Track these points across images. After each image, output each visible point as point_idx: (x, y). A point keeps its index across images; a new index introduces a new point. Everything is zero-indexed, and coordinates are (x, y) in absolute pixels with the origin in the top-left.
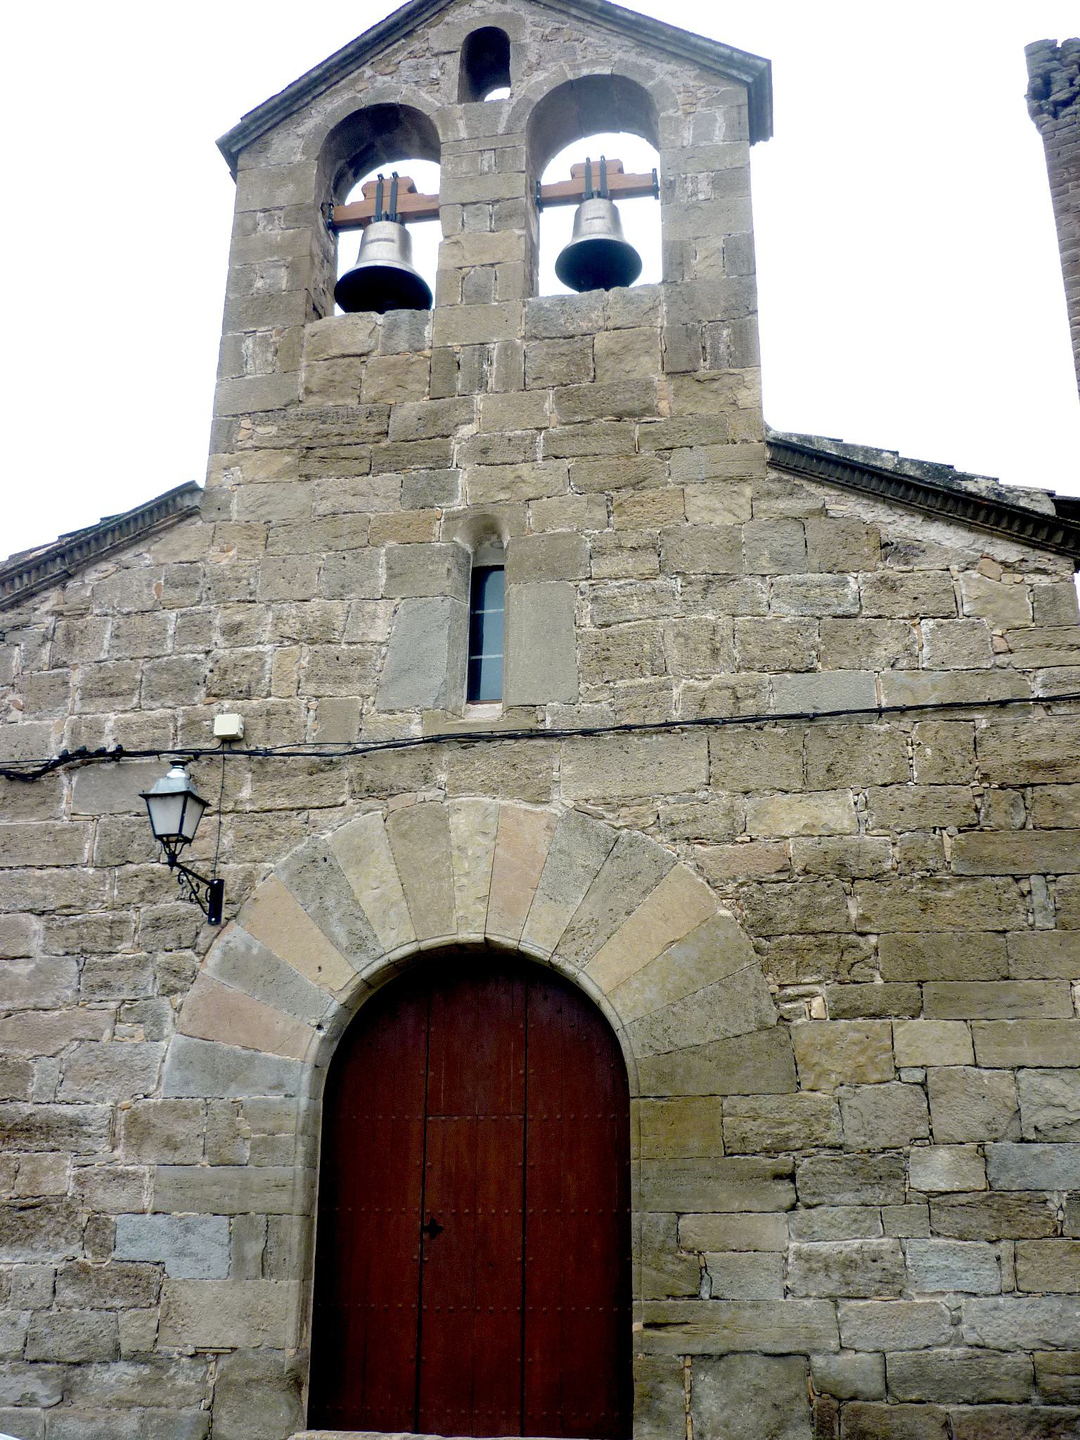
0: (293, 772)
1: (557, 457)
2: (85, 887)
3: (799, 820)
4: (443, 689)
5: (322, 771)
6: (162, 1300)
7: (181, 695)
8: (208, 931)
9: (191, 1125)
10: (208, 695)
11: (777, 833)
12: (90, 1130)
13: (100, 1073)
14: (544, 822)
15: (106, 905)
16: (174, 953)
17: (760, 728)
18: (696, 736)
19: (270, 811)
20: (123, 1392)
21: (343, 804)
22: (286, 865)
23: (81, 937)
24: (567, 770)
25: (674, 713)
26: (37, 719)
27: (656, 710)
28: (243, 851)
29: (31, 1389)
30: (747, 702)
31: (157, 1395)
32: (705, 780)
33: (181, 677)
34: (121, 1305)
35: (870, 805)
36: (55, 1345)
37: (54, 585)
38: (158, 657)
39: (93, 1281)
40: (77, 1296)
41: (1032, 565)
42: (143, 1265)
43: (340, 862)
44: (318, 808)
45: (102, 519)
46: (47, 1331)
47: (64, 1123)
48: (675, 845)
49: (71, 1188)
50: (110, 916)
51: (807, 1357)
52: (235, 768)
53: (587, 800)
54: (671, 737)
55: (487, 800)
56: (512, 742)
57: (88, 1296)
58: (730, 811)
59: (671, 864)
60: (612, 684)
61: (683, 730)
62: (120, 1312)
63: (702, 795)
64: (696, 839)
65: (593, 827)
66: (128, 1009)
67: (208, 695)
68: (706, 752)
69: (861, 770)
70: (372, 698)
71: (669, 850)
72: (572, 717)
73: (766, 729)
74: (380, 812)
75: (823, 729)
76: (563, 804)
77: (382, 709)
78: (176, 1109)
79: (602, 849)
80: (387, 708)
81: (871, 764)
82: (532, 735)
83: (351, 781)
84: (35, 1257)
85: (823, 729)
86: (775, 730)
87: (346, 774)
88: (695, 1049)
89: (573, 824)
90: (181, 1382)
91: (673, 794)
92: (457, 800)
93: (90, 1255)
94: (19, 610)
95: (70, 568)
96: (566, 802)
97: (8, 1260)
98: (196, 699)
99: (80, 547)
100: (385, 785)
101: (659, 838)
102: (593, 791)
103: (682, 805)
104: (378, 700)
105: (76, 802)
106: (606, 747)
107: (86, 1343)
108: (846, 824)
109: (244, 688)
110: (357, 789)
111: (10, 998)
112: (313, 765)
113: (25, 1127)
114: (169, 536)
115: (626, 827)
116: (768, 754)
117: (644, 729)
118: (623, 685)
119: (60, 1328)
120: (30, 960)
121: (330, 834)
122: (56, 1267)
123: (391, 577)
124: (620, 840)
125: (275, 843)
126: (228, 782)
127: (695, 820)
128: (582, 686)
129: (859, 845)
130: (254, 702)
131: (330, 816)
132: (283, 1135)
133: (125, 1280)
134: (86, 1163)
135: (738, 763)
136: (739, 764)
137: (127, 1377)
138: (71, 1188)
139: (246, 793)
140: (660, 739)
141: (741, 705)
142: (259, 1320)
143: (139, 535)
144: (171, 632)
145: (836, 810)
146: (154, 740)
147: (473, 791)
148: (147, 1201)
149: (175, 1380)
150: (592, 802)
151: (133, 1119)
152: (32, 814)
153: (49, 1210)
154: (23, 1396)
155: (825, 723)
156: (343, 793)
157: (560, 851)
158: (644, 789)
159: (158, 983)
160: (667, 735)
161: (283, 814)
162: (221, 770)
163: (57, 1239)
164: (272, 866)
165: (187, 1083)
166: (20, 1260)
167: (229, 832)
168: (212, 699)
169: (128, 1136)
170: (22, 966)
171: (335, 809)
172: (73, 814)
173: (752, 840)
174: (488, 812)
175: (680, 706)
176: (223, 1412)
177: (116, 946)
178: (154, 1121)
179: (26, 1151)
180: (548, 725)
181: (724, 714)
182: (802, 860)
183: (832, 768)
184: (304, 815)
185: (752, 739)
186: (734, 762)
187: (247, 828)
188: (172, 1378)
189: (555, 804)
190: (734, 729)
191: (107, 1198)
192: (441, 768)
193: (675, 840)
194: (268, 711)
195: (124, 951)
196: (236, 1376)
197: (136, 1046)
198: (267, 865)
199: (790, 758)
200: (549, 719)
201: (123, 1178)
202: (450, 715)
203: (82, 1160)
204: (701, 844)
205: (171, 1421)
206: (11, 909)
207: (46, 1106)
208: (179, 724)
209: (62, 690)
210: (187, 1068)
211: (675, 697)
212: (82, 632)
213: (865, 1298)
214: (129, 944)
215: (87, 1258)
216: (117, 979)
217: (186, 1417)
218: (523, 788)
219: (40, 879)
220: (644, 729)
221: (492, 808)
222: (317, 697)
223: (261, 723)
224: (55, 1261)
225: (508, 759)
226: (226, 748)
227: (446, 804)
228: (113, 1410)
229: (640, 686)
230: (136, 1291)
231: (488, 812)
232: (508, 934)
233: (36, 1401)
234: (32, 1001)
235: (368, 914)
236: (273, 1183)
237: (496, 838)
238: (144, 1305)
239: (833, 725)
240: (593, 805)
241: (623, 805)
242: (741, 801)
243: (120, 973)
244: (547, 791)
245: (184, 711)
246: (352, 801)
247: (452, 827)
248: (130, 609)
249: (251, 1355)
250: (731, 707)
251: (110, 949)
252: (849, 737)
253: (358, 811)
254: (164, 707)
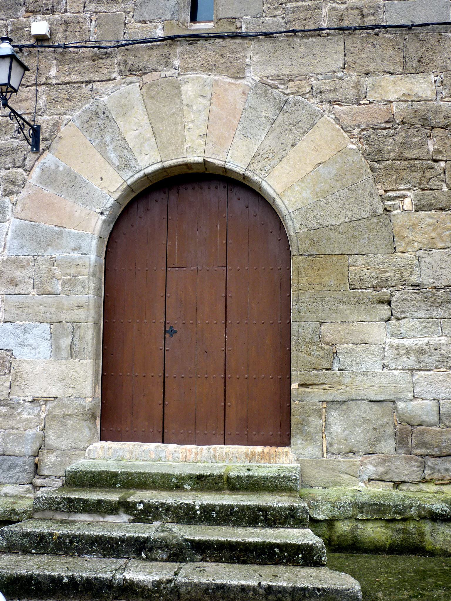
0: (82, 59)
3: (400, 90)
4: (177, 8)
5: (101, 58)
6: (12, 370)
7: (9, 12)
8: (31, 157)
10: (27, 11)
11: (386, 99)
14: (241, 90)
17: (376, 34)
18: (336, 38)
19: (68, 83)
21: (115, 79)
22: (79, 116)
24: (256, 58)
25: (323, 23)
27: (312, 22)
28: (52, 108)
30: (369, 18)
31: (12, 423)
32: (342, 65)
35: (444, 82)
43: (113, 114)
44: (98, 81)
48: (322, 105)
51: (394, 402)
52: (45, 57)
53: (268, 77)
54: (321, 39)
55: (205, 76)
56: (221, 40)
58: (357, 85)
59: (320, 116)
60: (284, 5)
61: (328, 34)
63: (340, 74)
64: (335, 102)
65: (271, 93)
67: (27, 11)
68: (343, 48)
69: (440, 62)
70: (131, 14)
71: (318, 108)
72: (259, 26)
73: (381, 34)
74: (138, 84)
75: (417, 35)
76: (253, 79)
77: (138, 19)
79: (277, 107)
80: (141, 19)
81: (446, 57)
82: (234, 36)
83: (119, 65)
85: (417, 35)
86: (386, 35)
87: (116, 61)
89: (259, 91)
90: (25, 416)
91: (321, 74)
92: (186, 76)
96: (254, 78)
98: (19, 14)
100: (141, 67)
101: (312, 101)
102: (271, 71)
103: (327, 81)
104: (135, 14)
106: (280, 44)
108: (429, 94)
109: (50, 7)
110: (123, 69)
112: (95, 54)
115: (292, 93)
116: (381, 50)
117: (305, 33)
118: (291, 6)
121: (106, 98)
124: (289, 101)
125: (72, 103)
126: (41, 65)
127: (335, 90)
128: (265, 6)
129: (437, 107)
130: (57, 16)
131: (106, 86)
132: (81, 277)
135: (363, 56)
136: (363, 56)
139: (53, 72)
140: (314, 40)
141: (366, 19)
142: (70, 382)
145: (423, 85)
147: (196, 70)
149: (22, 415)
150: (271, 78)
155: (417, 31)
156: (115, 72)
157: (251, 108)
158: (303, 70)
160: (318, 37)
161: (76, 85)
162: (37, 58)
164: (71, 117)
165: (22, 247)
167: (43, 96)
168: (29, 14)
171: (110, 82)
173: (370, 103)
174: (206, 83)
175: (327, 19)
176: (50, 432)
180: (244, 30)
181: (355, 25)
182: (401, 115)
183: (422, 59)
184: (90, 86)
185: (372, 40)
186: (360, 55)
187: (54, 94)
189: (247, 79)
190: (360, 34)
192: (176, 57)
193: (322, 102)
194: (65, 21)
196: (57, 412)
198: (67, 117)
199: (395, 53)
200: (244, 27)
202: (181, 25)
204: (338, 105)
208: (9, 30)
210: (21, 238)
211: (324, 14)
213: (429, 370)
217: (29, 435)
218: (228, 69)
220: (305, 33)
221: (208, 81)
222: (96, 13)
223: (62, 29)
225: (218, 51)
226: (39, 44)
227: (179, 79)
229: (302, 7)
231: (206, 83)
232: (218, 158)
235: (131, 146)
236: (76, 305)
237: (211, 99)
239: (423, 33)
240: (272, 80)
241: (290, 80)
242: (363, 79)
244: (243, 71)
245: (12, 22)
246: (120, 77)
247: (183, 93)
250: (359, 20)
252: (433, 41)
253: (124, 83)
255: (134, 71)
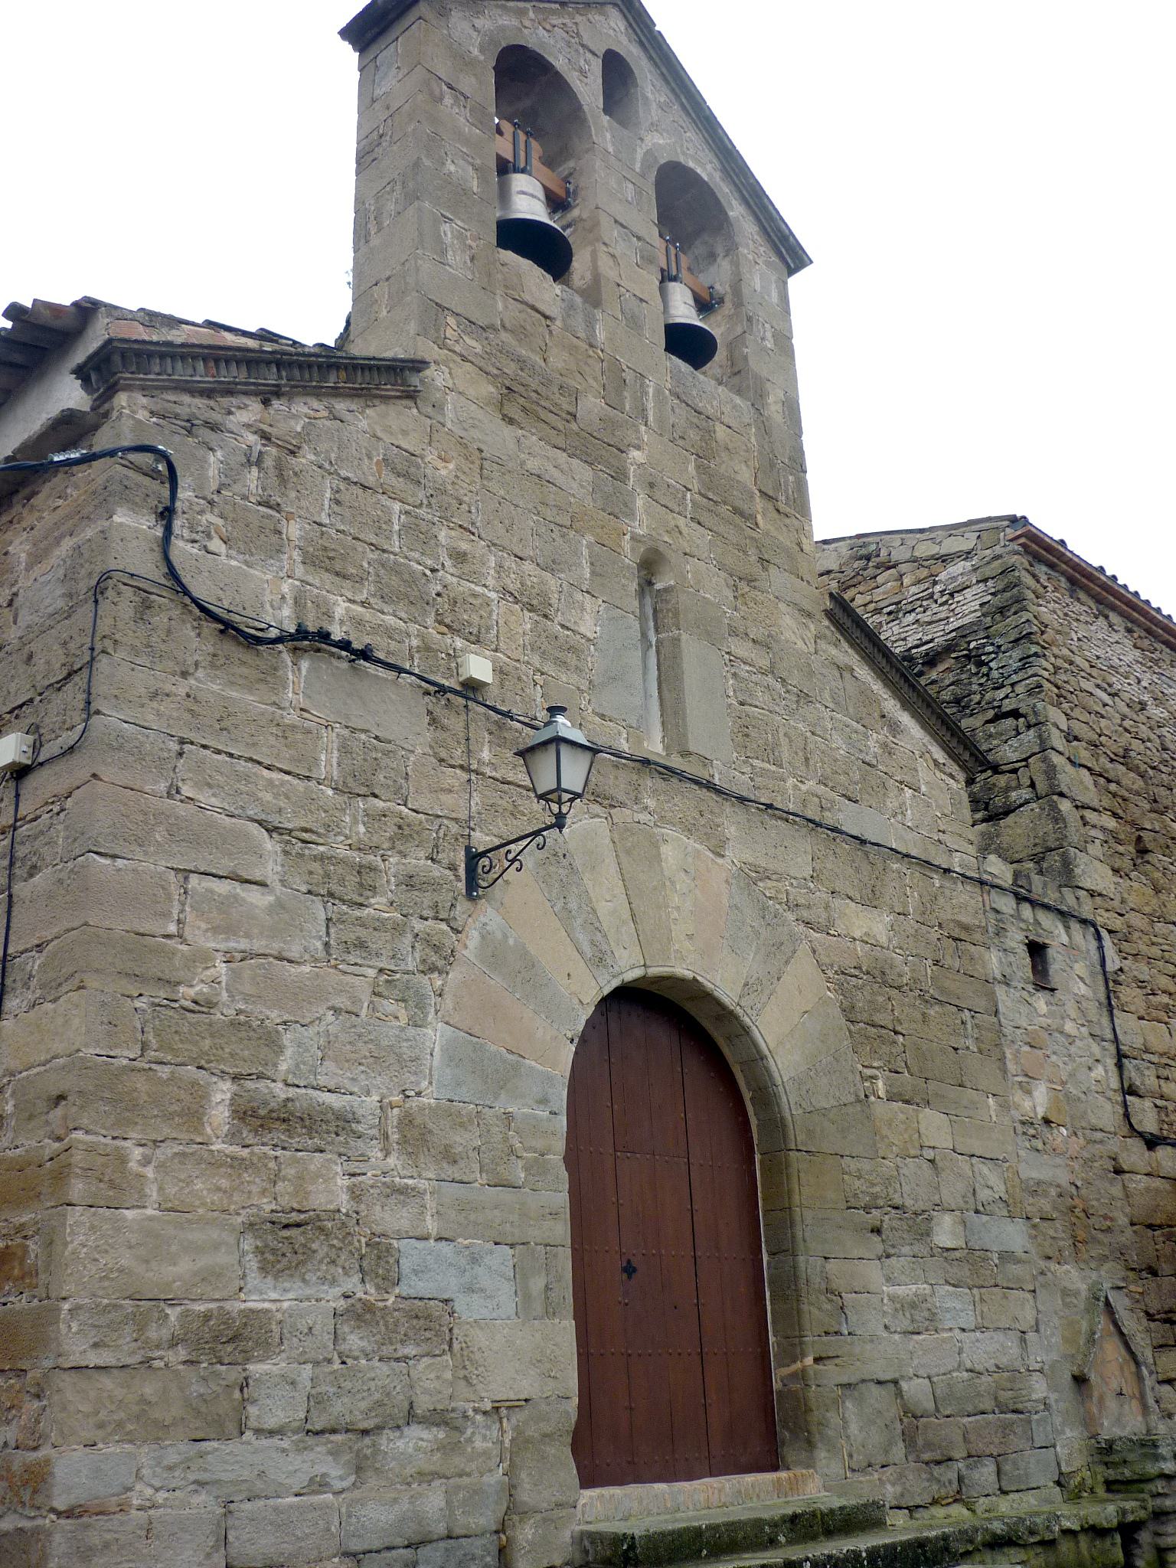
1: (699, 523)
2: (326, 811)
6: (456, 1346)
8: (463, 905)
9: (467, 1136)
12: (360, 1128)
13: (365, 1057)
15: (349, 841)
16: (430, 922)
20: (423, 1463)
23: (327, 875)
26: (246, 563)
29: (320, 1469)
31: (458, 1461)
33: (410, 587)
34: (414, 1353)
36: (340, 1409)
37: (256, 394)
38: (384, 551)
39: (381, 1323)
40: (364, 1344)
41: (948, 771)
42: (432, 1302)
43: (578, 863)
45: (262, 329)
46: (332, 1390)
47: (330, 1116)
49: (344, 1202)
50: (356, 857)
51: (895, 1382)
56: (696, 787)
57: (376, 1342)
62: (411, 1363)
66: (387, 981)
78: (449, 1112)
84: (308, 1291)
85: (866, 854)
88: (823, 1112)
90: (479, 1444)
93: (373, 1291)
94: (212, 403)
95: (285, 385)
97: (274, 1296)
99: (300, 366)
104: (593, 700)
105: (307, 696)
107: (380, 1404)
111: (248, 936)
113: (282, 1116)
114: (383, 407)
119: (348, 1385)
120: (266, 890)
122: (334, 1305)
123: (593, 573)
132: (552, 1157)
133: (415, 1322)
134: (358, 1171)
137: (424, 1444)
138: (344, 1202)
142: (548, 1366)
143: (362, 389)
144: (396, 528)
146: (388, 653)
147: (674, 826)
148: (431, 1225)
149: (473, 1442)
151: (407, 1121)
152: (250, 690)
153: (321, 1229)
154: (311, 1479)
159: (417, 955)
163: (332, 1269)
166: (291, 1295)
169: (404, 1141)
170: (259, 896)
172: (302, 709)
176: (523, 1475)
177: (368, 898)
178: (430, 1126)
179: (284, 1148)
188: (470, 1440)
191: (391, 1218)
195: (376, 906)
196: (531, 1432)
197: (402, 1029)
201: (402, 1193)
203: (353, 1167)
205: (475, 1492)
206: (237, 812)
207: (303, 1091)
209: (274, 538)
210: (457, 1066)
212: (296, 474)
213: (918, 1333)
214: (384, 900)
215: (368, 1292)
216: (378, 941)
217: (490, 1485)
219: (270, 782)
224: (332, 1298)
228: (414, 1486)
230: (428, 1334)
232: (708, 977)
233: (327, 1484)
234: (275, 947)
235: (605, 926)
236: (548, 1211)
238: (437, 1352)
243: (375, 933)
245: (418, 630)
247: (663, 856)
248: (350, 475)
249: (543, 1406)
251: (360, 900)
254: (395, 616)
255: (598, 796)
